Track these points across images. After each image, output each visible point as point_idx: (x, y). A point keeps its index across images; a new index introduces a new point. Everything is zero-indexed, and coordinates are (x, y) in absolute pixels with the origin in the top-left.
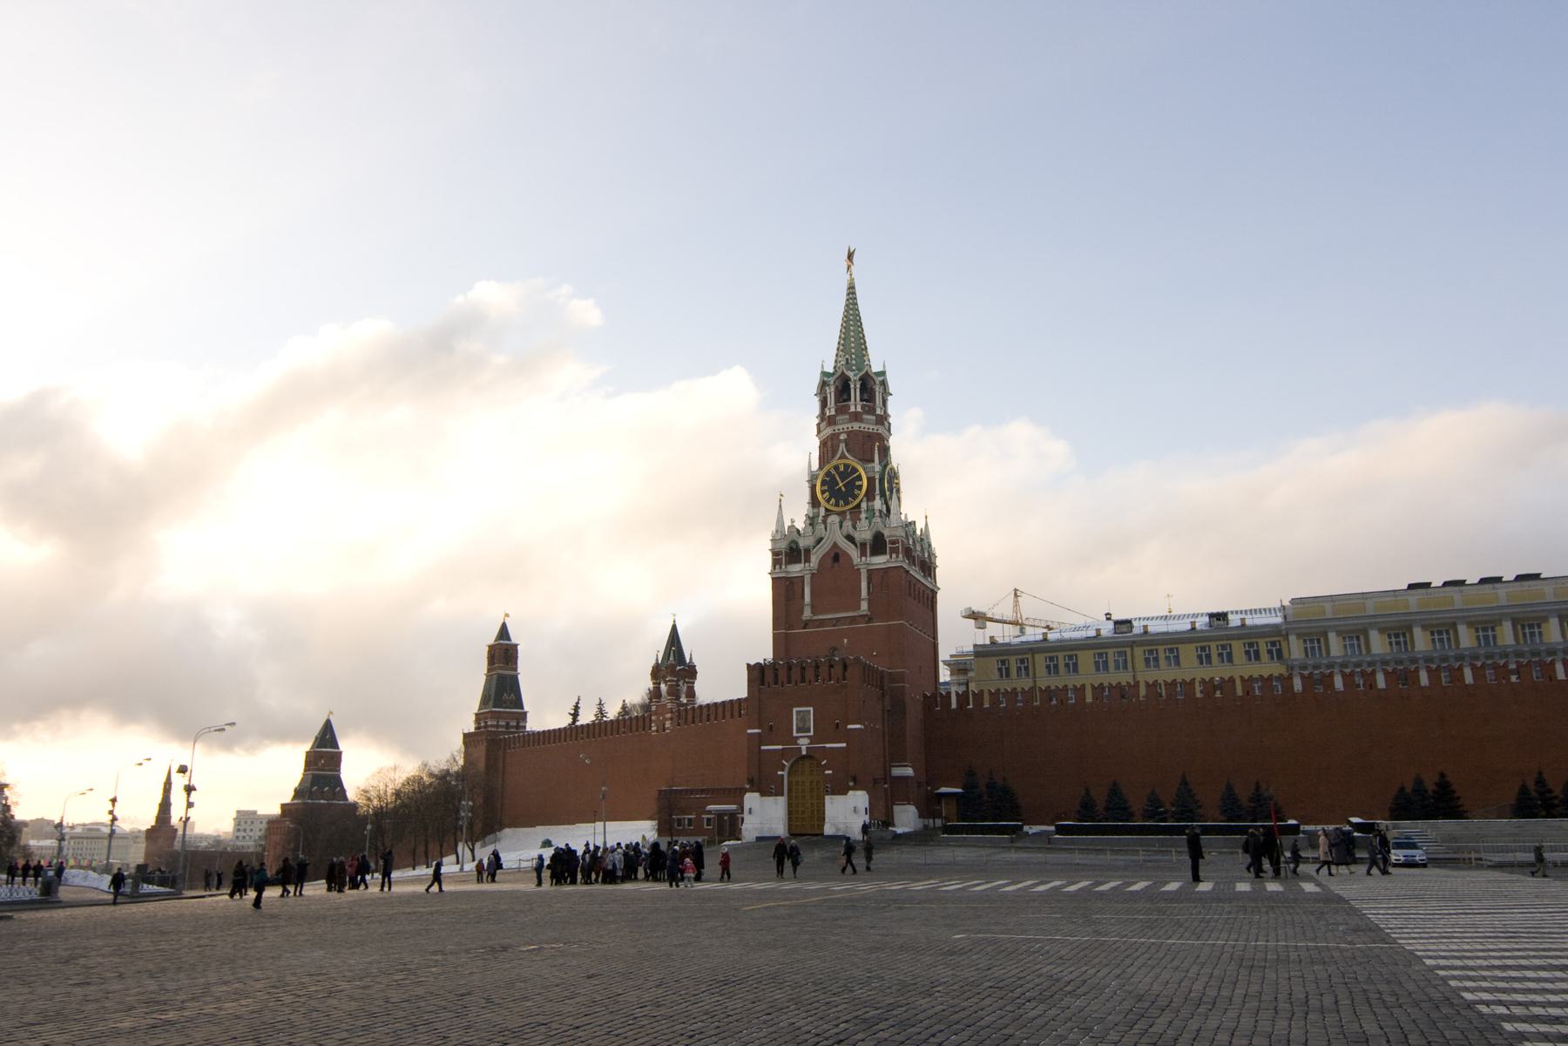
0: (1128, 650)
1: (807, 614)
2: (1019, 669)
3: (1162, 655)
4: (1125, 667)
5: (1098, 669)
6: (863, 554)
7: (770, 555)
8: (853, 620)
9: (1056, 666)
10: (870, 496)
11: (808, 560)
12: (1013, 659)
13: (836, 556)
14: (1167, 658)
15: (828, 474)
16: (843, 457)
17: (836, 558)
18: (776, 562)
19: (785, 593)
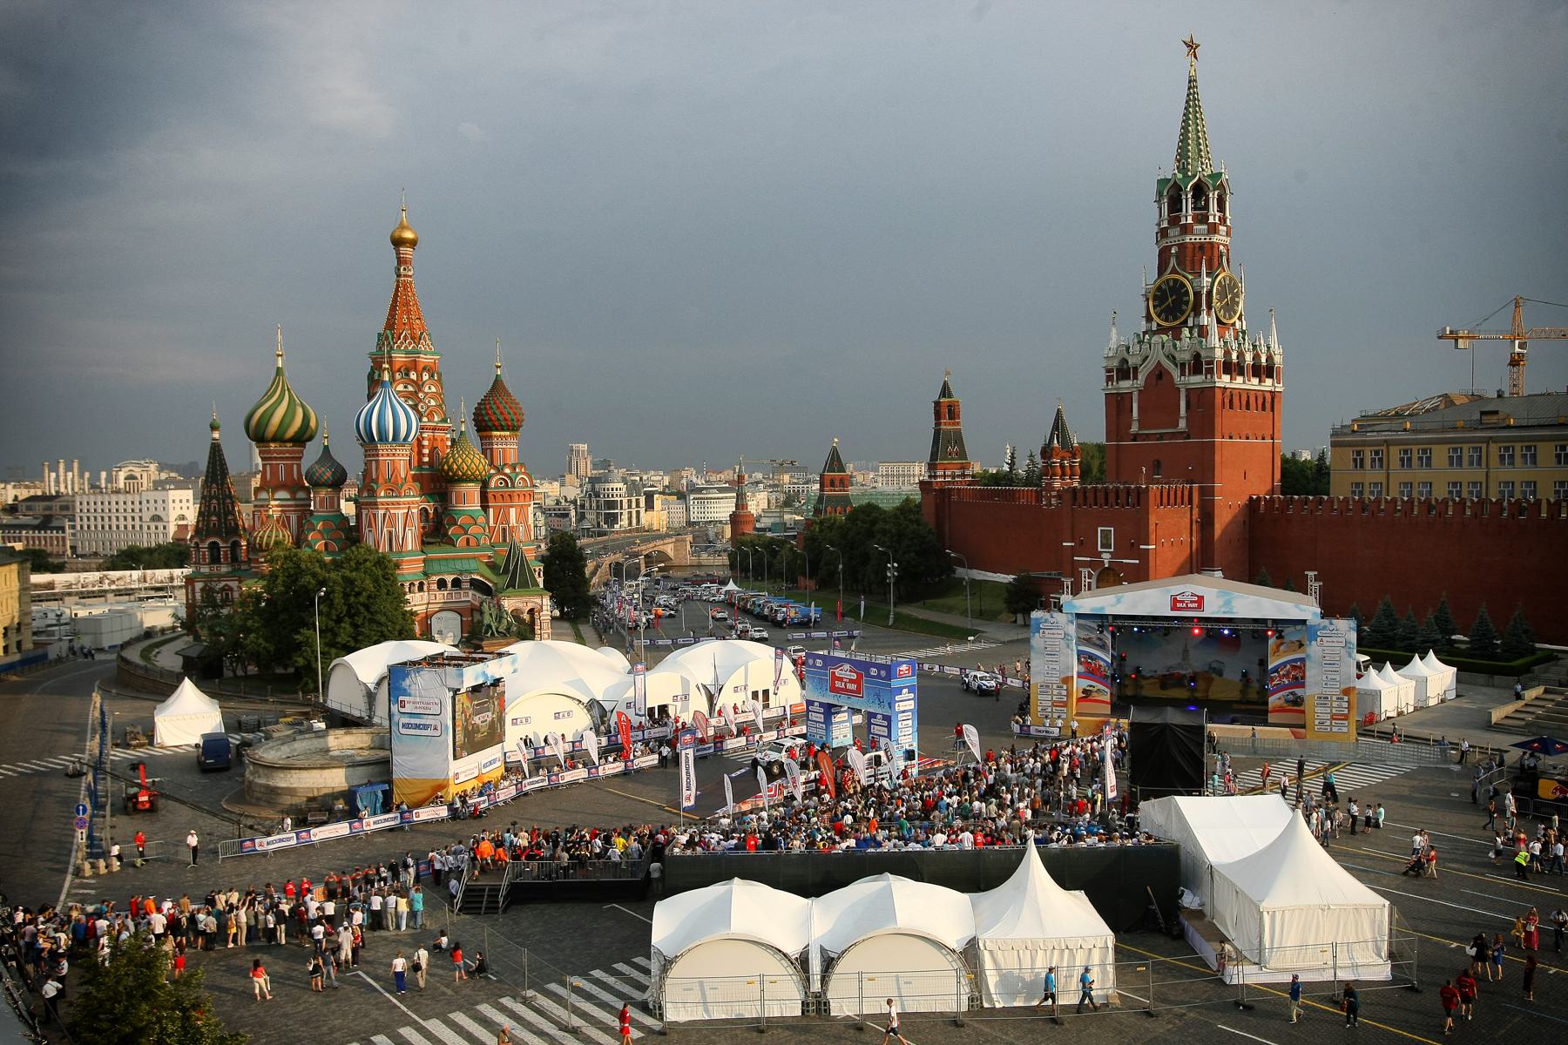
0: (1484, 446)
1: (1134, 428)
2: (1373, 460)
3: (1518, 454)
4: (1479, 464)
5: (1451, 464)
6: (1183, 374)
7: (1103, 374)
8: (1174, 435)
9: (1410, 459)
10: (1197, 311)
11: (1135, 378)
12: (1367, 450)
13: (1159, 374)
14: (1524, 456)
15: (1159, 288)
16: (1174, 271)
17: (1160, 376)
18: (1109, 379)
19: (1117, 405)
